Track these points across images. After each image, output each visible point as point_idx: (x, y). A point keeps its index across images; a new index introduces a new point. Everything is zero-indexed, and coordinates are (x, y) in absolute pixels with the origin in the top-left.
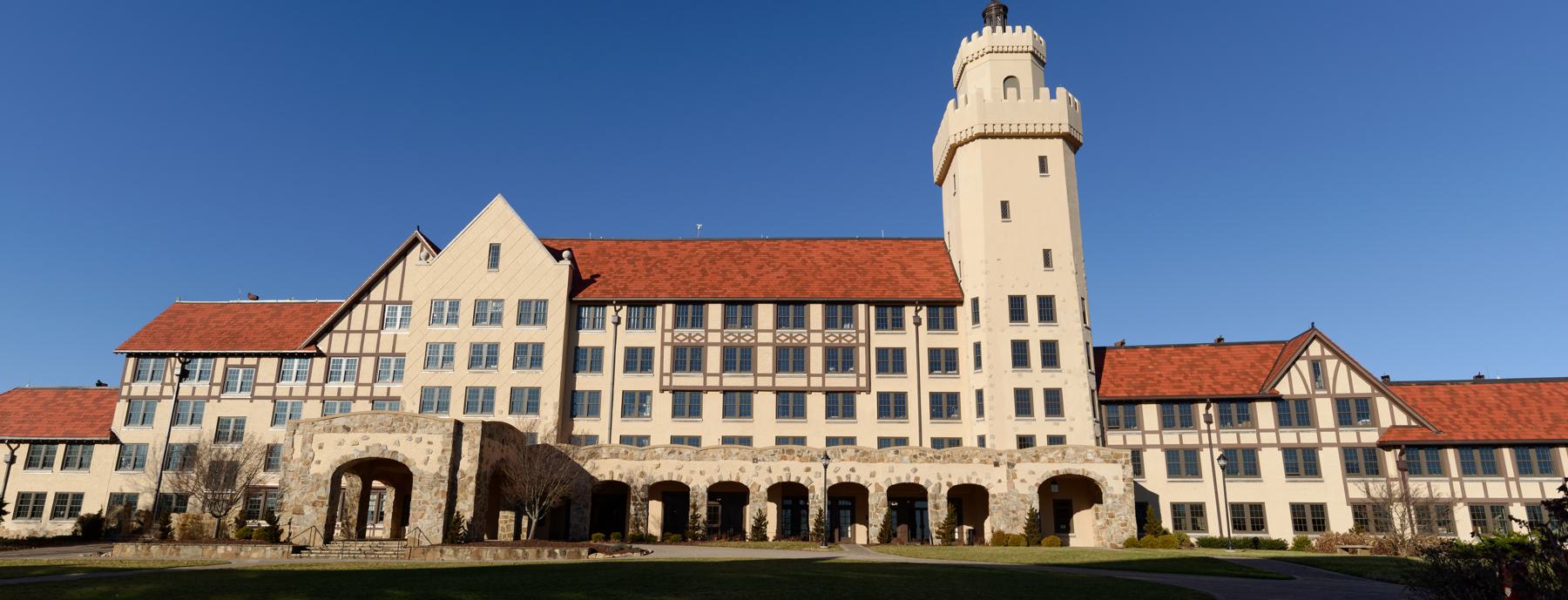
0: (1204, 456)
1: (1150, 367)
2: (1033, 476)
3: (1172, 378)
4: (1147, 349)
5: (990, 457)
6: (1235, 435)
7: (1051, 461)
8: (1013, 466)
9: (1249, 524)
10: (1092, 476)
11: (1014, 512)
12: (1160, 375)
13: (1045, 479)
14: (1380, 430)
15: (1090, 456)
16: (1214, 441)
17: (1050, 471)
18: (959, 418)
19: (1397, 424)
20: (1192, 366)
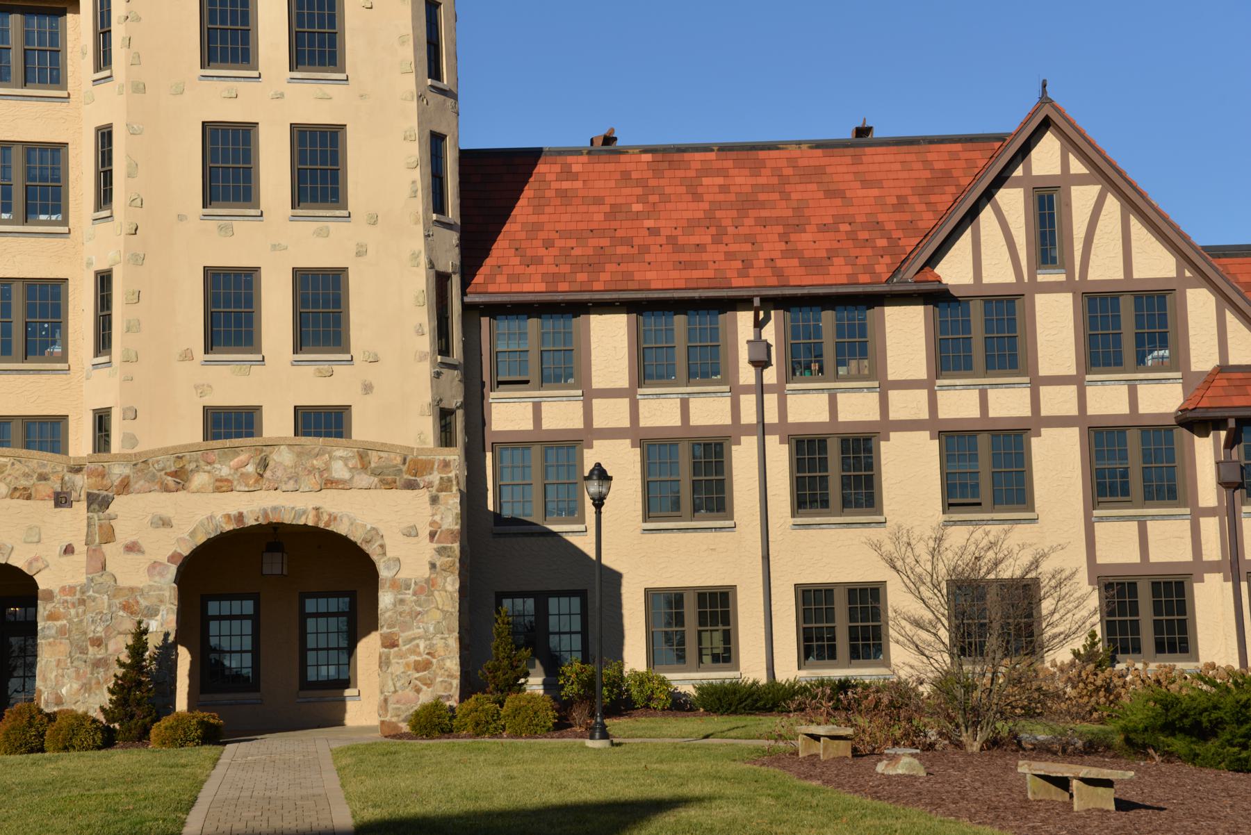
0: (743, 457)
1: (637, 207)
2: (164, 531)
3: (681, 240)
4: (648, 157)
5: (43, 478)
6: (825, 397)
7: (222, 486)
8: (105, 503)
9: (843, 643)
10: (342, 529)
11: (97, 642)
12: (653, 232)
13: (201, 539)
14: (1188, 379)
15: (339, 471)
16: (771, 417)
17: (219, 516)
18: (64, 358)
19: (1234, 360)
20: (746, 203)
